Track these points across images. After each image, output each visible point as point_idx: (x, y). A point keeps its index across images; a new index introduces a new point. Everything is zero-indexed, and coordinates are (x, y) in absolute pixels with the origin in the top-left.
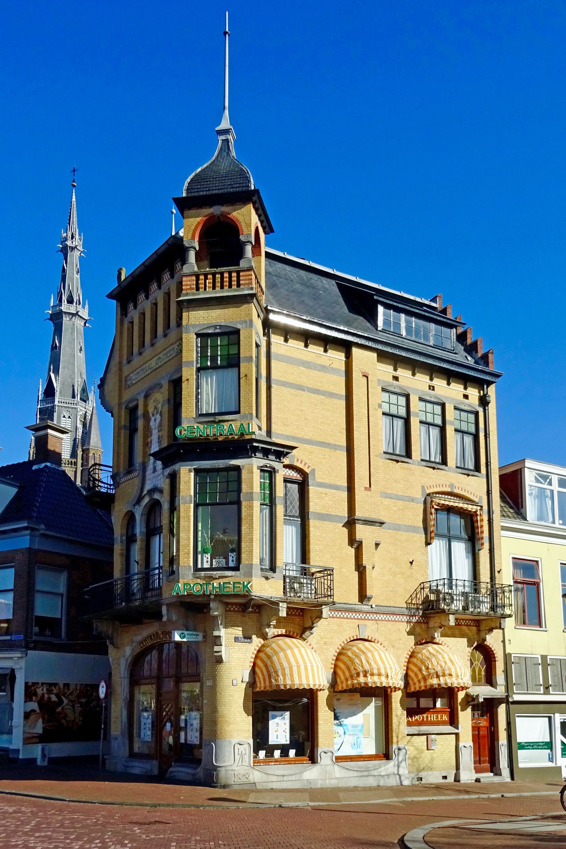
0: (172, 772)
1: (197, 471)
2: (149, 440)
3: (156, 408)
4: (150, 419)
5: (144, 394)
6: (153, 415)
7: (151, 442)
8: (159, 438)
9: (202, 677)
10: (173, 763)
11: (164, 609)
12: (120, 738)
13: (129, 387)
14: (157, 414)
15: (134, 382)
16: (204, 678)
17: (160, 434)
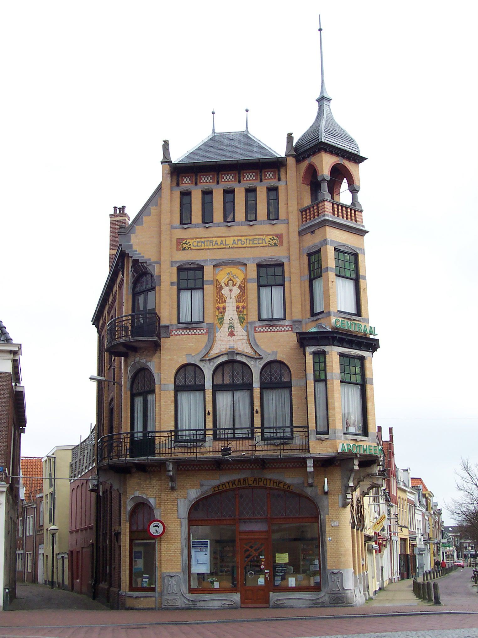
0: (277, 600)
1: (341, 355)
2: (221, 305)
3: (230, 280)
4: (221, 288)
5: (214, 263)
6: (227, 285)
7: (224, 308)
8: (238, 308)
9: (324, 519)
10: (271, 593)
11: (310, 463)
12: (181, 575)
13: (184, 249)
14: (234, 285)
15: (193, 248)
16: (327, 520)
17: (241, 305)
